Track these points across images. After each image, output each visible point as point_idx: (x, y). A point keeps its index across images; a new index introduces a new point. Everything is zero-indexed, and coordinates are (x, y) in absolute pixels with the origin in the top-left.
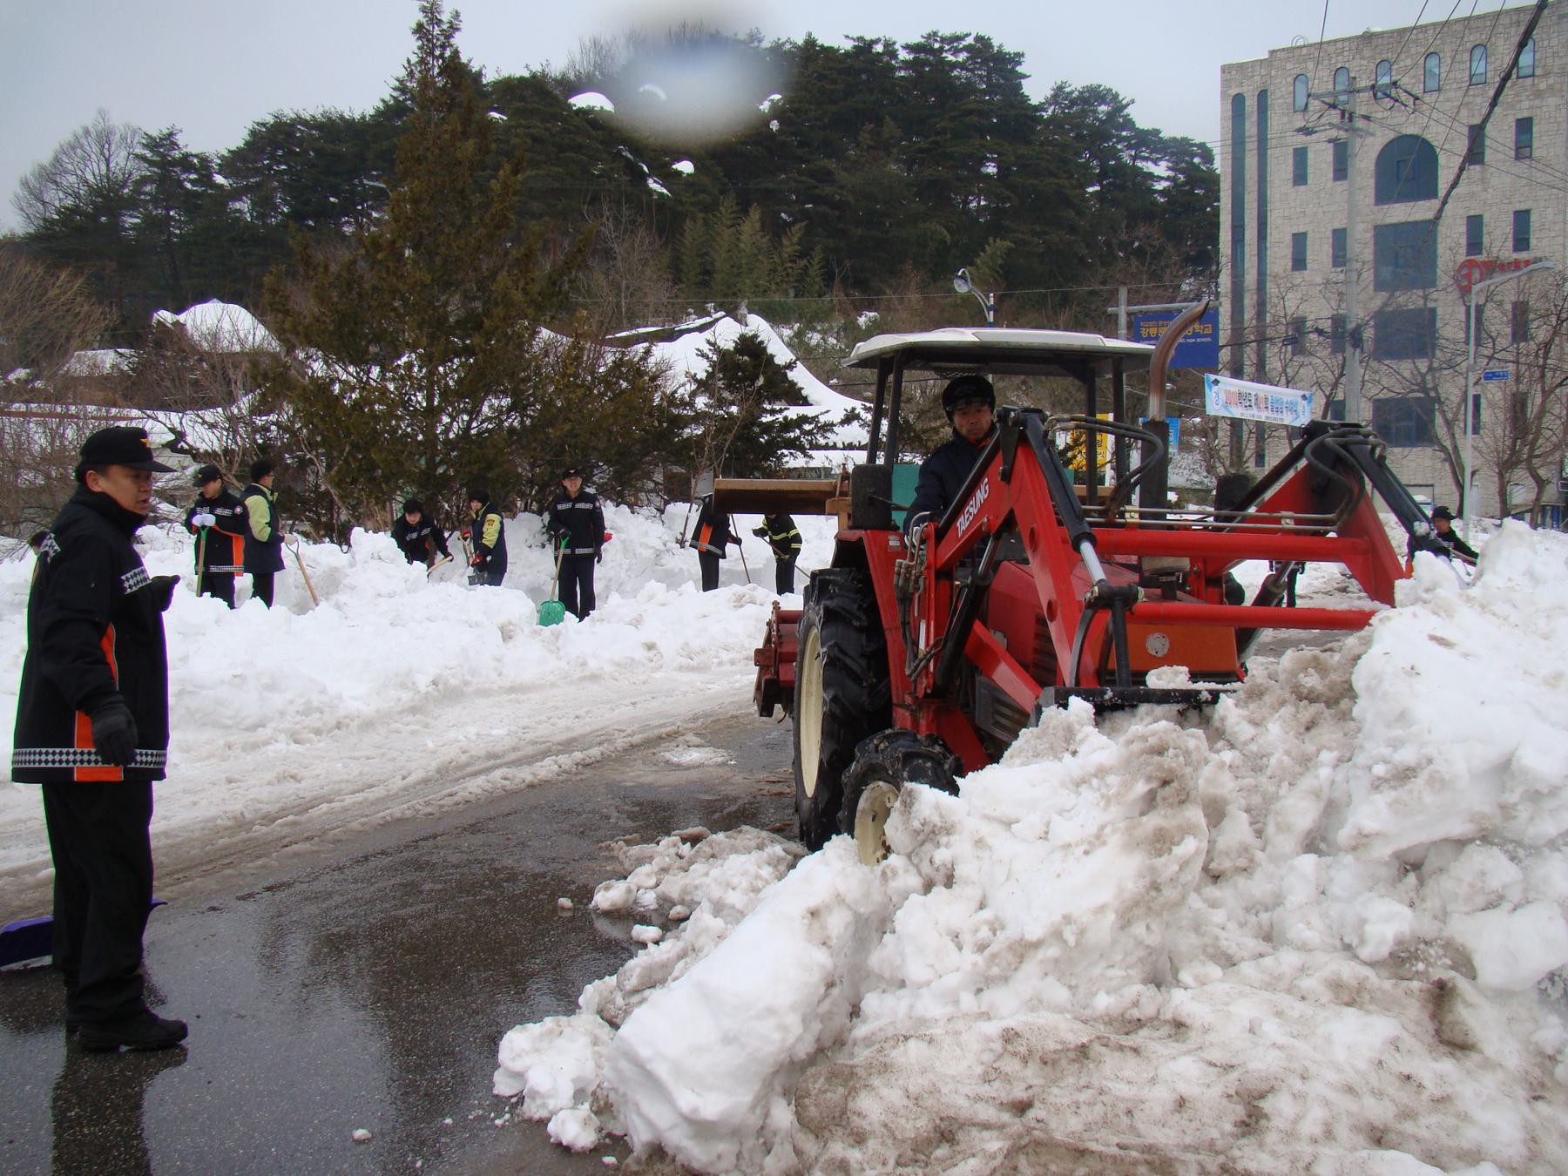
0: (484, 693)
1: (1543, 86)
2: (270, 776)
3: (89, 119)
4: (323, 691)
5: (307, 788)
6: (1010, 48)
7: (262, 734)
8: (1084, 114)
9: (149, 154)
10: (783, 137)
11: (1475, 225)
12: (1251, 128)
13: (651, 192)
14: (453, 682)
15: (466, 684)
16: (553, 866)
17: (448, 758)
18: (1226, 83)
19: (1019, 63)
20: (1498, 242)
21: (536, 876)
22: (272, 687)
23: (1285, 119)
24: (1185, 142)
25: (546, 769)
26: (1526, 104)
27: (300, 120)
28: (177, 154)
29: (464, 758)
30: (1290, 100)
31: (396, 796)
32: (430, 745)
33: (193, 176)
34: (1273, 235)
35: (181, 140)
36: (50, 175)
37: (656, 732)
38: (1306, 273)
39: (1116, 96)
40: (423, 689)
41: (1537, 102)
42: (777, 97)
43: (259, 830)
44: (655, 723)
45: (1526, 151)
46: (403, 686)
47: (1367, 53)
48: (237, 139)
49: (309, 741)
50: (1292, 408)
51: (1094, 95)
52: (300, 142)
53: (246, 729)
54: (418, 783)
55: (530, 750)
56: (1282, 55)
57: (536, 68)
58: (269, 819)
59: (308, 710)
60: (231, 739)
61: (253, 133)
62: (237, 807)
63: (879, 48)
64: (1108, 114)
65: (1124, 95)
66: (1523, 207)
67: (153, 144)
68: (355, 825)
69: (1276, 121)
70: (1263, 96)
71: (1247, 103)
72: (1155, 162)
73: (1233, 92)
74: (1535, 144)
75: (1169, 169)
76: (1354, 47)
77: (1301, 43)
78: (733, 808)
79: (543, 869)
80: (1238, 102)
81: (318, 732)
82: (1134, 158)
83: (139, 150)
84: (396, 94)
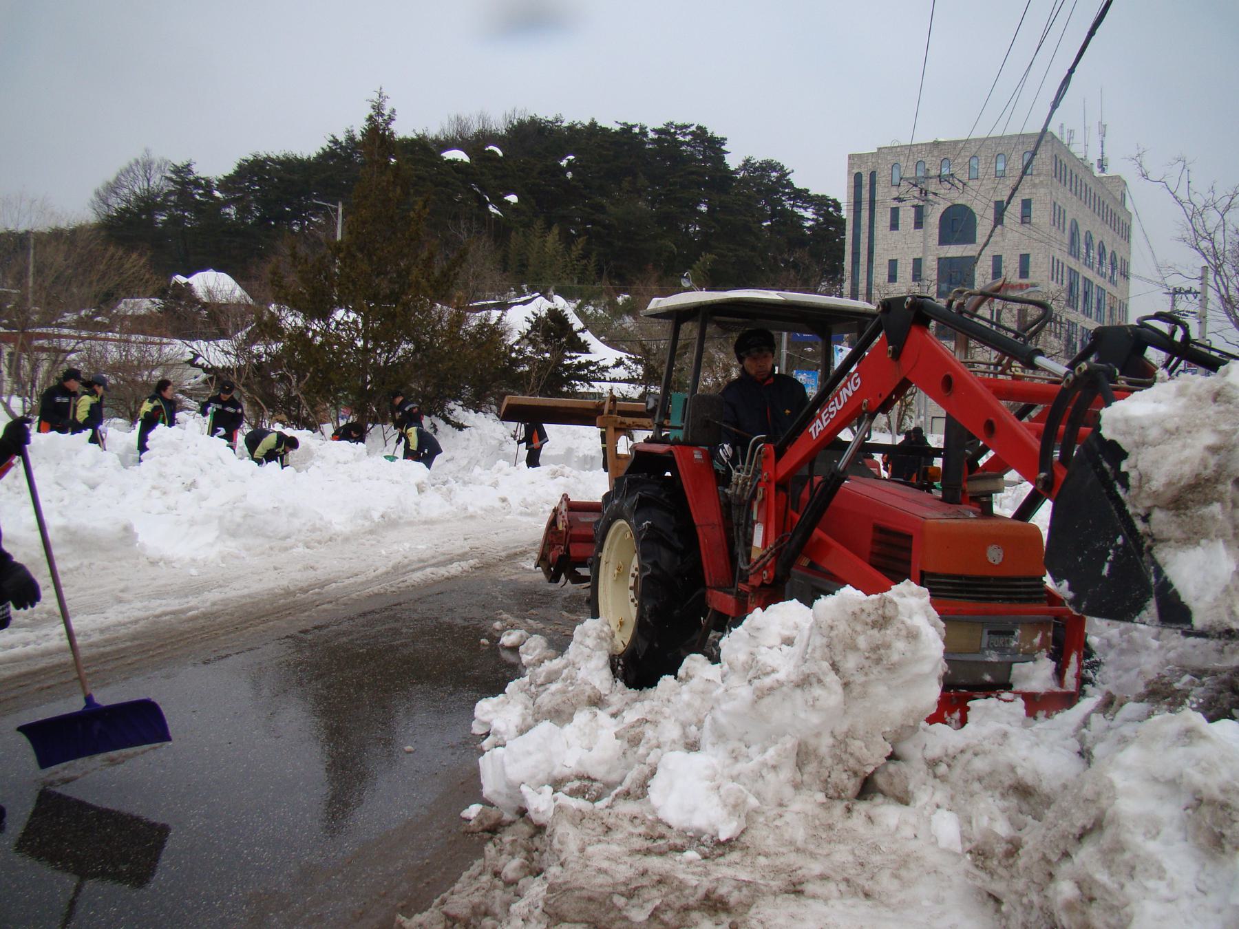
0: (410, 524)
1: (1037, 181)
2: (299, 566)
3: (139, 154)
4: (321, 519)
5: (321, 574)
6: (718, 135)
7: (289, 542)
8: (762, 177)
9: (174, 177)
10: (574, 183)
11: (997, 260)
12: (865, 195)
13: (490, 214)
14: (393, 516)
15: (400, 518)
16: (472, 622)
17: (398, 561)
18: (851, 166)
19: (724, 144)
21: (464, 628)
22: (293, 515)
23: (886, 190)
24: (824, 197)
25: (455, 569)
26: (1027, 191)
27: (269, 159)
28: (191, 177)
29: (406, 561)
31: (371, 581)
32: (384, 552)
33: (201, 192)
35: (194, 168)
36: (113, 188)
37: (513, 551)
38: (896, 284)
39: (783, 167)
40: (376, 520)
41: (1034, 190)
42: (571, 157)
43: (300, 596)
44: (511, 545)
45: (1027, 219)
46: (365, 518)
47: (936, 153)
48: (229, 169)
49: (314, 547)
51: (769, 166)
52: (269, 173)
53: (280, 539)
54: (382, 574)
55: (441, 558)
56: (885, 151)
57: (420, 132)
58: (304, 591)
59: (314, 529)
60: (272, 544)
61: (240, 166)
62: (284, 583)
63: (636, 130)
64: (777, 178)
65: (788, 167)
66: (1025, 252)
67: (177, 171)
68: (354, 596)
70: (873, 175)
71: (864, 178)
72: (805, 209)
73: (856, 171)
74: (1033, 215)
75: (814, 214)
76: (928, 148)
77: (896, 144)
78: (567, 595)
79: (466, 624)
80: (858, 178)
81: (320, 542)
82: (793, 206)
83: (169, 174)
84: (331, 145)
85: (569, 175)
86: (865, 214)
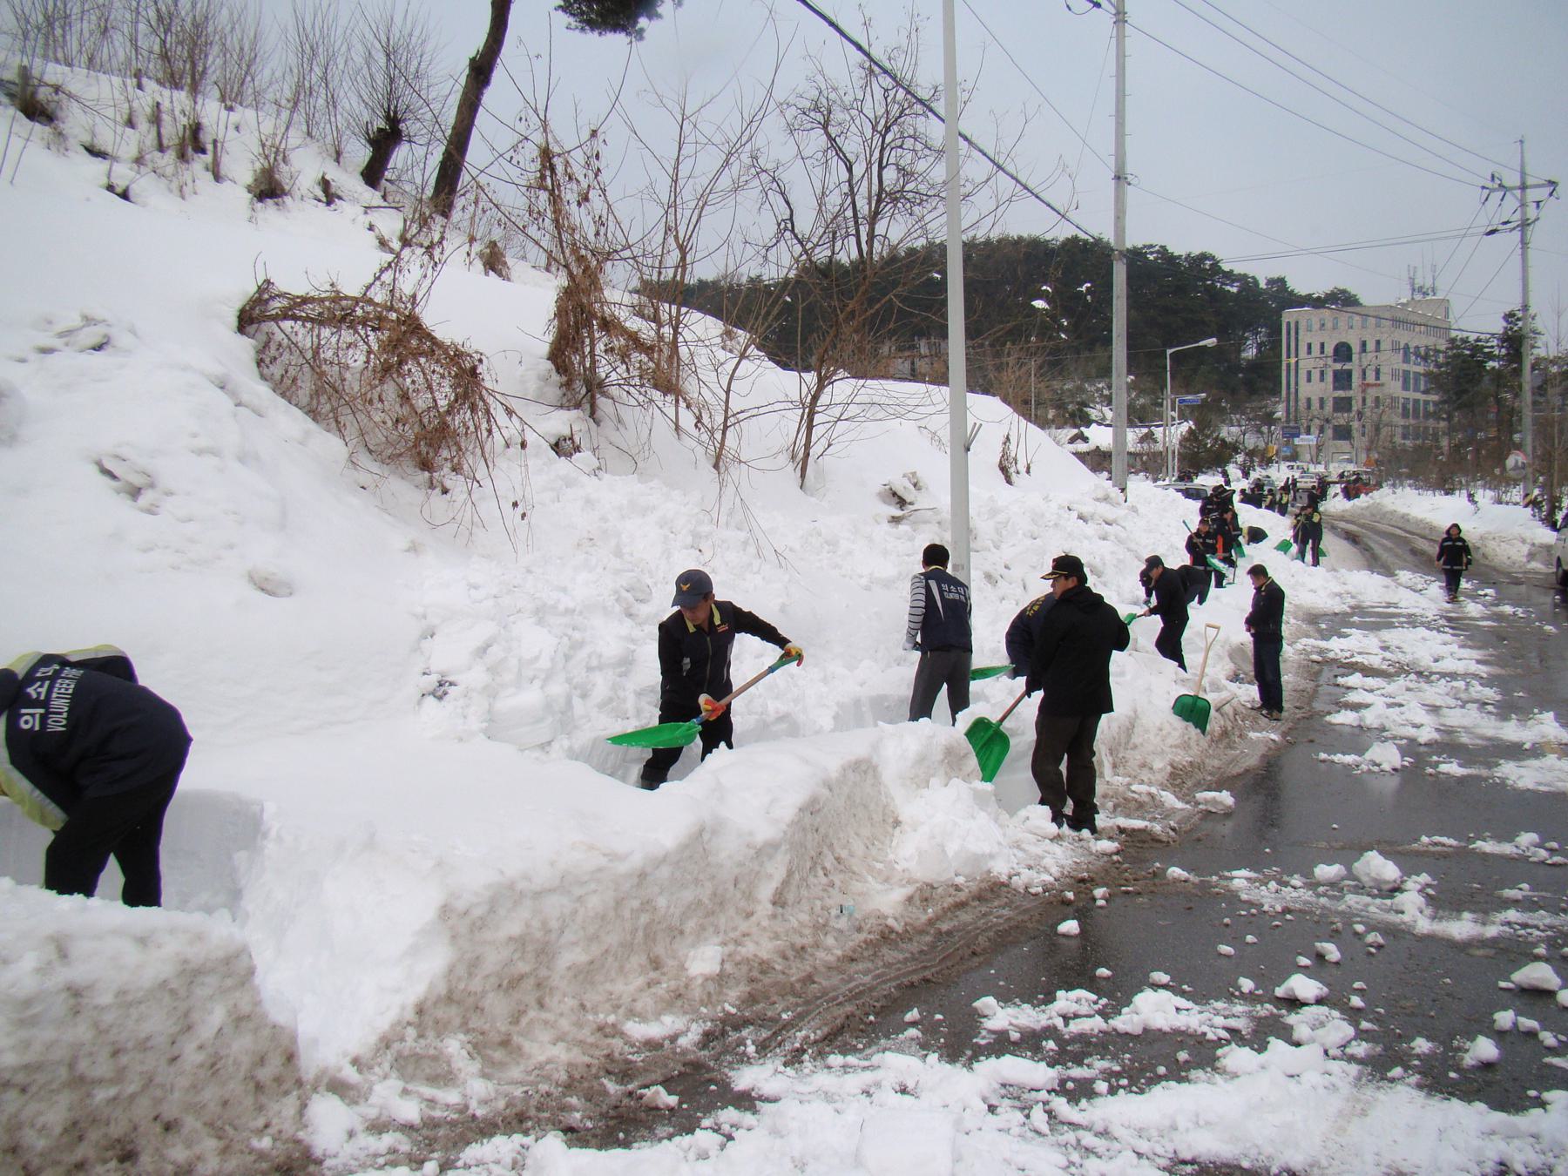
20: (1371, 378)
24: (1245, 276)
51: (1203, 257)
65: (1218, 256)
69: (1301, 332)
70: (1297, 323)
85: (1089, 297)
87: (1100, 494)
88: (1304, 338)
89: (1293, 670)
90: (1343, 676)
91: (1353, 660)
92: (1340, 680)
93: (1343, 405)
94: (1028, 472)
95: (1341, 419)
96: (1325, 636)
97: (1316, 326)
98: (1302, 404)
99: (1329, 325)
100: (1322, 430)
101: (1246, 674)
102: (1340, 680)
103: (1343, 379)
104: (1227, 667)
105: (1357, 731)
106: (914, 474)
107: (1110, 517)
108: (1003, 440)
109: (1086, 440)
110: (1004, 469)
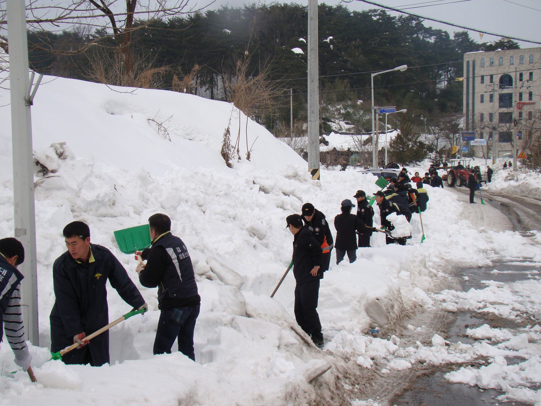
23: (479, 69)
30: (480, 64)
34: (476, 95)
38: (484, 103)
42: (331, 38)
47: (497, 55)
50: (483, 142)
51: (412, 17)
57: (224, 5)
69: (477, 68)
85: (331, 46)
86: (471, 80)
87: (291, 172)
88: (479, 72)
89: (428, 321)
90: (474, 326)
91: (485, 310)
92: (469, 332)
93: (506, 118)
94: (248, 158)
95: (504, 127)
96: (465, 287)
97: (487, 64)
98: (477, 118)
99: (496, 62)
100: (491, 136)
101: (380, 326)
102: (469, 332)
103: (506, 100)
104: (363, 321)
105: (474, 390)
106: (62, 144)
107: (288, 189)
108: (224, 132)
109: (326, 143)
110: (225, 156)
